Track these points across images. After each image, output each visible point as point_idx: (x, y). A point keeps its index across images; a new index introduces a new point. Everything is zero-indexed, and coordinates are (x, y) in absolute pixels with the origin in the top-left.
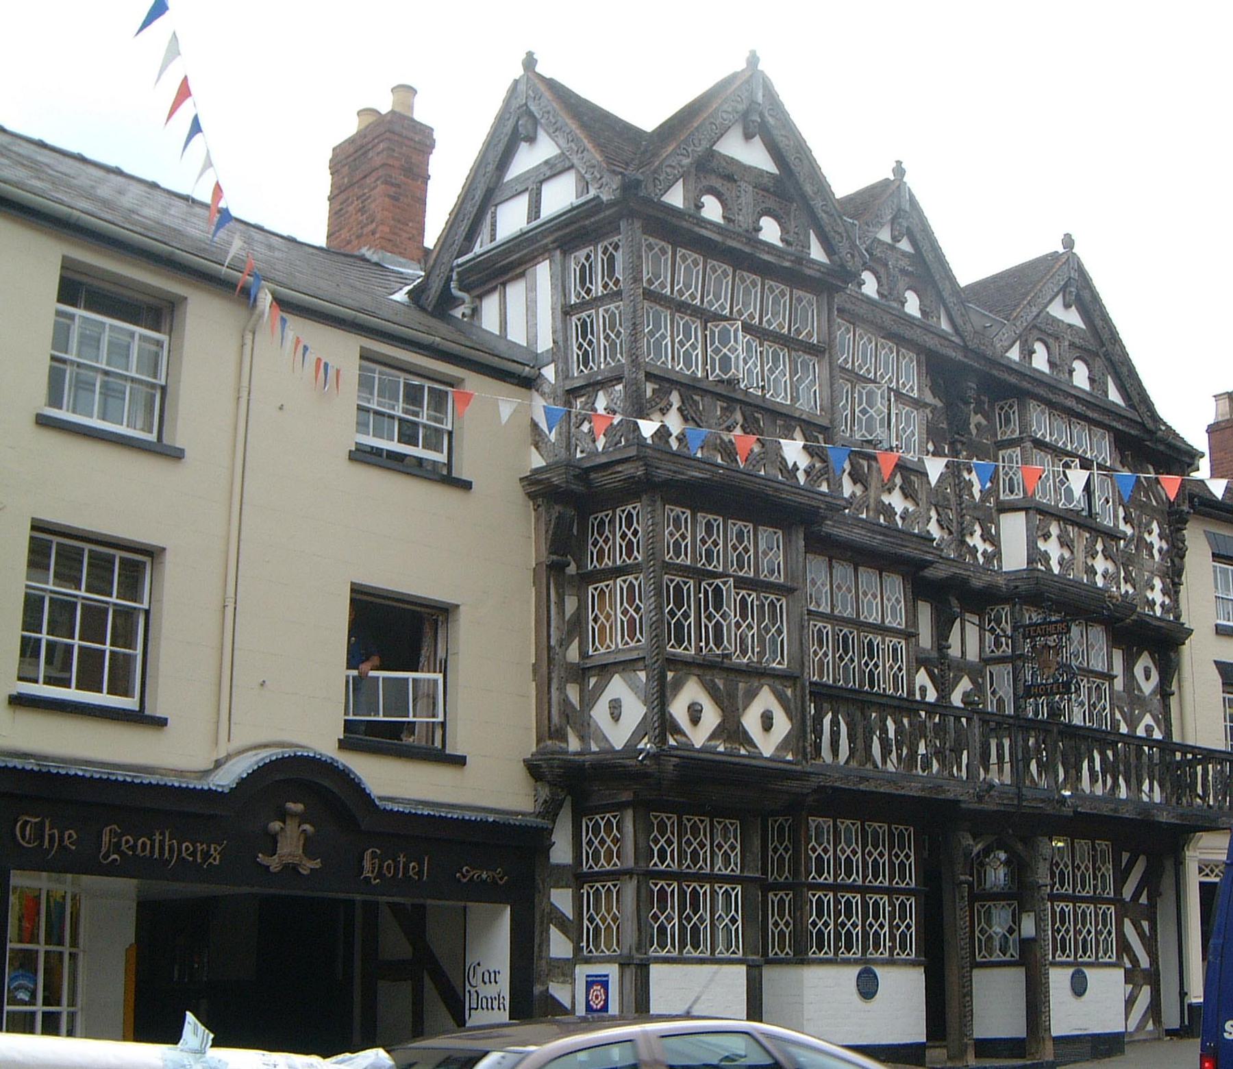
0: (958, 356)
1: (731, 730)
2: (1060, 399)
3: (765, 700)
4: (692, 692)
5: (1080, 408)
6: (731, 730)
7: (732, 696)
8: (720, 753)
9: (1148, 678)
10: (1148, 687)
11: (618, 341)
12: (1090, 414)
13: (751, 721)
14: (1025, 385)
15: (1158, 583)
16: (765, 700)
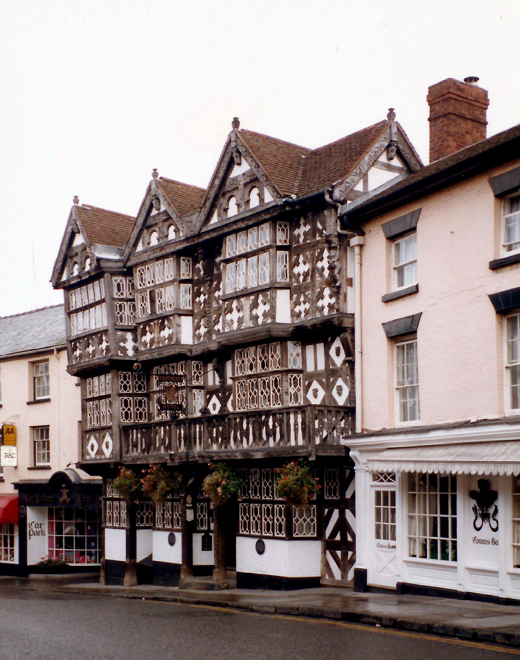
0: (185, 245)
1: (100, 452)
2: (235, 227)
3: (108, 438)
4: (93, 441)
5: (243, 225)
6: (100, 452)
7: (99, 439)
8: (98, 460)
9: (338, 354)
10: (339, 361)
11: (118, 310)
12: (250, 223)
13: (104, 447)
14: (214, 235)
15: (327, 292)
16: (108, 438)
